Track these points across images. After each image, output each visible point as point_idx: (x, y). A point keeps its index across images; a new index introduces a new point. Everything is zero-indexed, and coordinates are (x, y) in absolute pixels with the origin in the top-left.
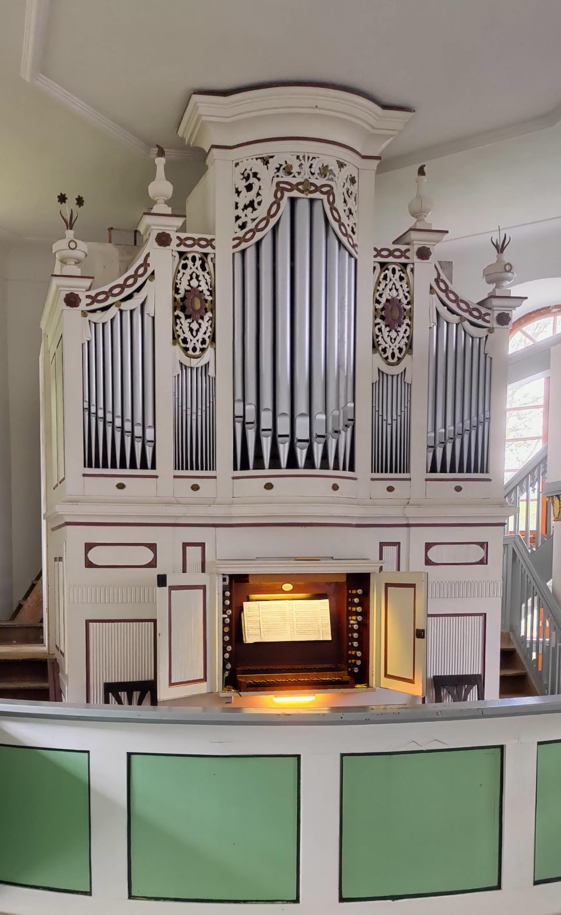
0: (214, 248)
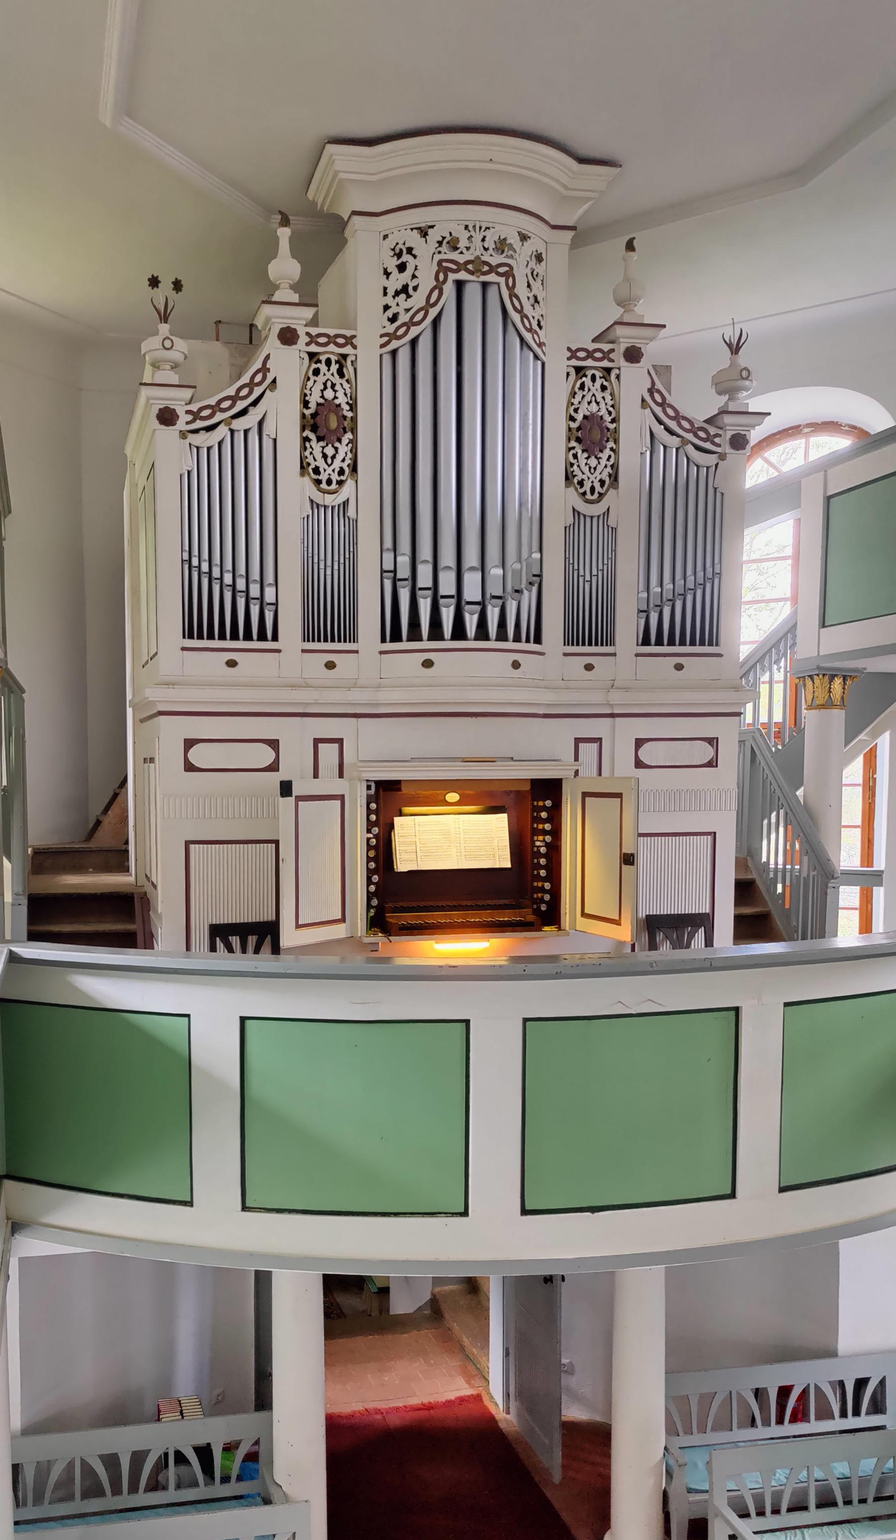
0: (355, 347)
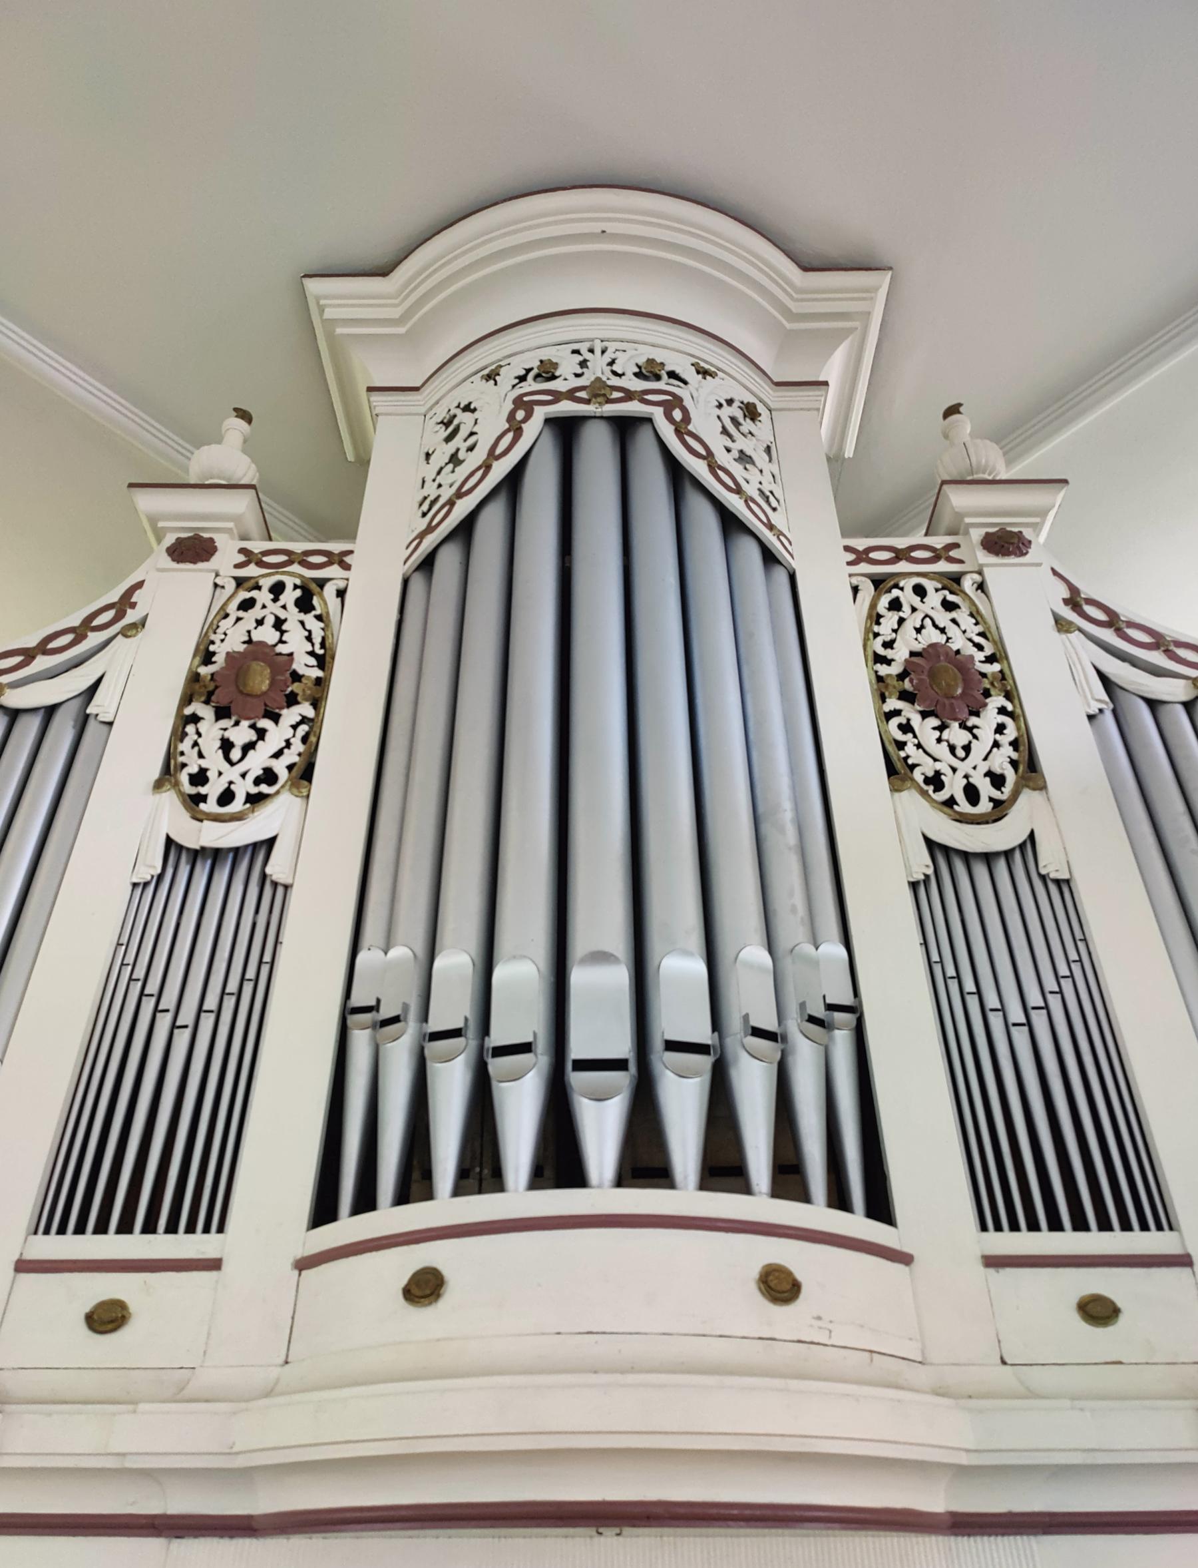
0: (347, 567)
